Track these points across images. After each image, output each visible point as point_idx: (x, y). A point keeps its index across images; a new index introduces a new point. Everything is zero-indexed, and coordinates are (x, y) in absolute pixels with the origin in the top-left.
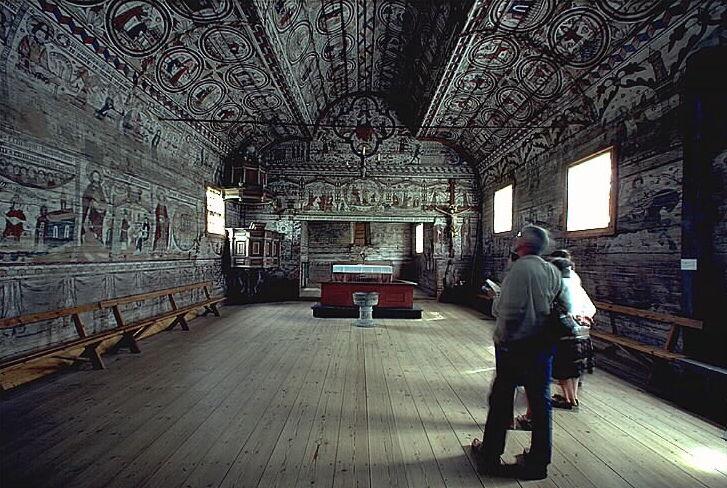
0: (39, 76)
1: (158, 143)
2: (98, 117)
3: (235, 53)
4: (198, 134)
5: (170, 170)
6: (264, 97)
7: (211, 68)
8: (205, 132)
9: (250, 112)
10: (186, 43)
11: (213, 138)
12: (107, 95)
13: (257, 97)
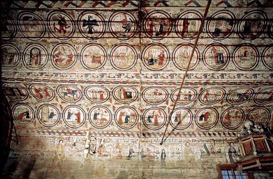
0: (105, 155)
1: (165, 156)
2: (128, 159)
3: (160, 94)
4: (194, 138)
5: (177, 168)
6: (208, 94)
7: (165, 107)
8: (200, 134)
9: (218, 104)
10: (144, 108)
11: (209, 134)
12: (129, 149)
13: (206, 97)
